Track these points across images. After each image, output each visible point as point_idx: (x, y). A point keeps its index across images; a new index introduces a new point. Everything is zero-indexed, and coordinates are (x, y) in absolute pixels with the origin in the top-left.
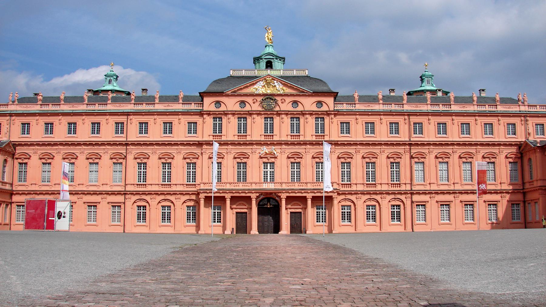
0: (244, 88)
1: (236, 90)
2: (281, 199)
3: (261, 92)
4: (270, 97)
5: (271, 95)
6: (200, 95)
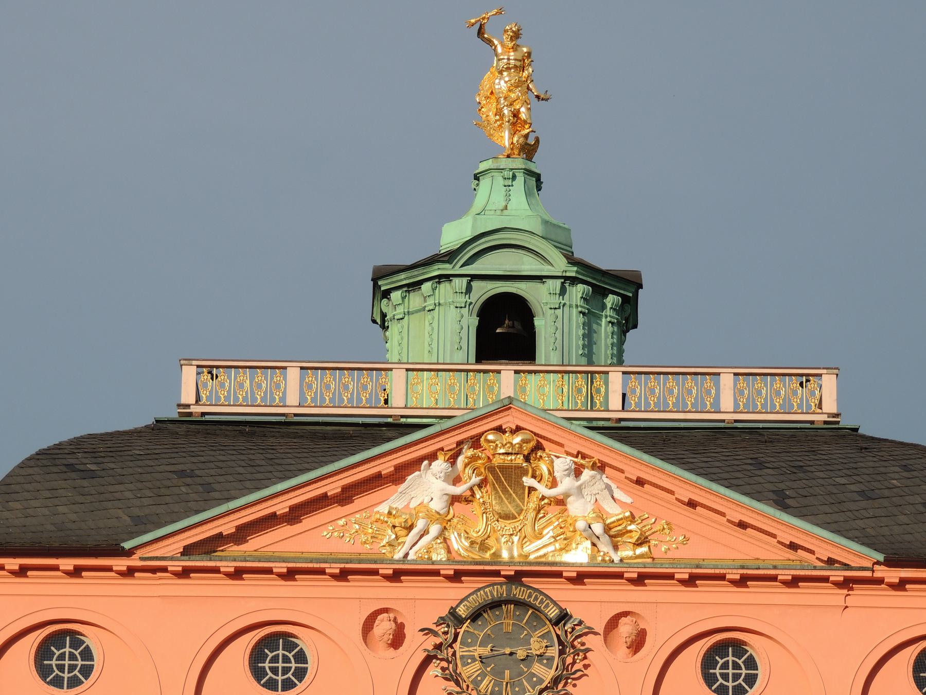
0: (295, 515)
1: (227, 527)
3: (440, 555)
4: (519, 593)
5: (517, 578)
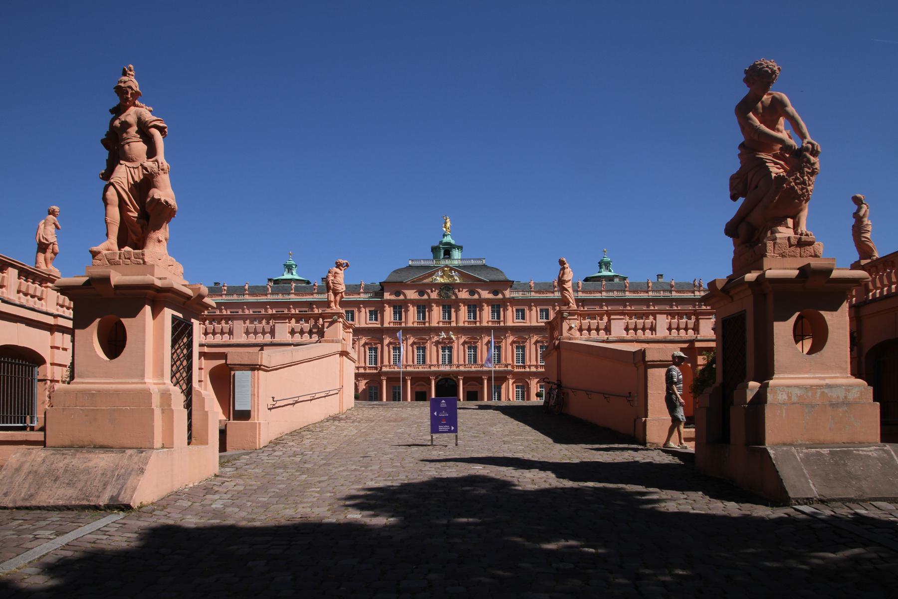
2: (459, 380)
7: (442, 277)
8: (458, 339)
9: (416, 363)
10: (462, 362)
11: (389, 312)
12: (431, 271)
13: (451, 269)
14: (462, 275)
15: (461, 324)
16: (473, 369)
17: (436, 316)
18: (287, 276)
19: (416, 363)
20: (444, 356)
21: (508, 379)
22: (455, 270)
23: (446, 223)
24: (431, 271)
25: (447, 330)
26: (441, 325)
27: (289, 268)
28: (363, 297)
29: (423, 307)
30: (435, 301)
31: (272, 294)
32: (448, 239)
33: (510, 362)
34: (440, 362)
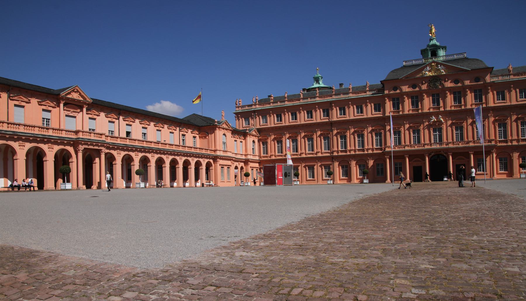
6: (382, 83)
7: (430, 71)
8: (446, 122)
9: (412, 143)
10: (450, 140)
11: (389, 106)
12: (421, 67)
13: (438, 63)
14: (447, 67)
15: (448, 109)
16: (461, 145)
17: (427, 104)
18: (316, 85)
19: (412, 143)
20: (435, 136)
21: (492, 153)
22: (441, 64)
23: (431, 30)
24: (421, 67)
25: (437, 114)
26: (431, 110)
27: (317, 80)
28: (369, 94)
29: (416, 99)
30: (425, 91)
31: (303, 99)
32: (434, 42)
33: (493, 138)
34: (433, 141)
